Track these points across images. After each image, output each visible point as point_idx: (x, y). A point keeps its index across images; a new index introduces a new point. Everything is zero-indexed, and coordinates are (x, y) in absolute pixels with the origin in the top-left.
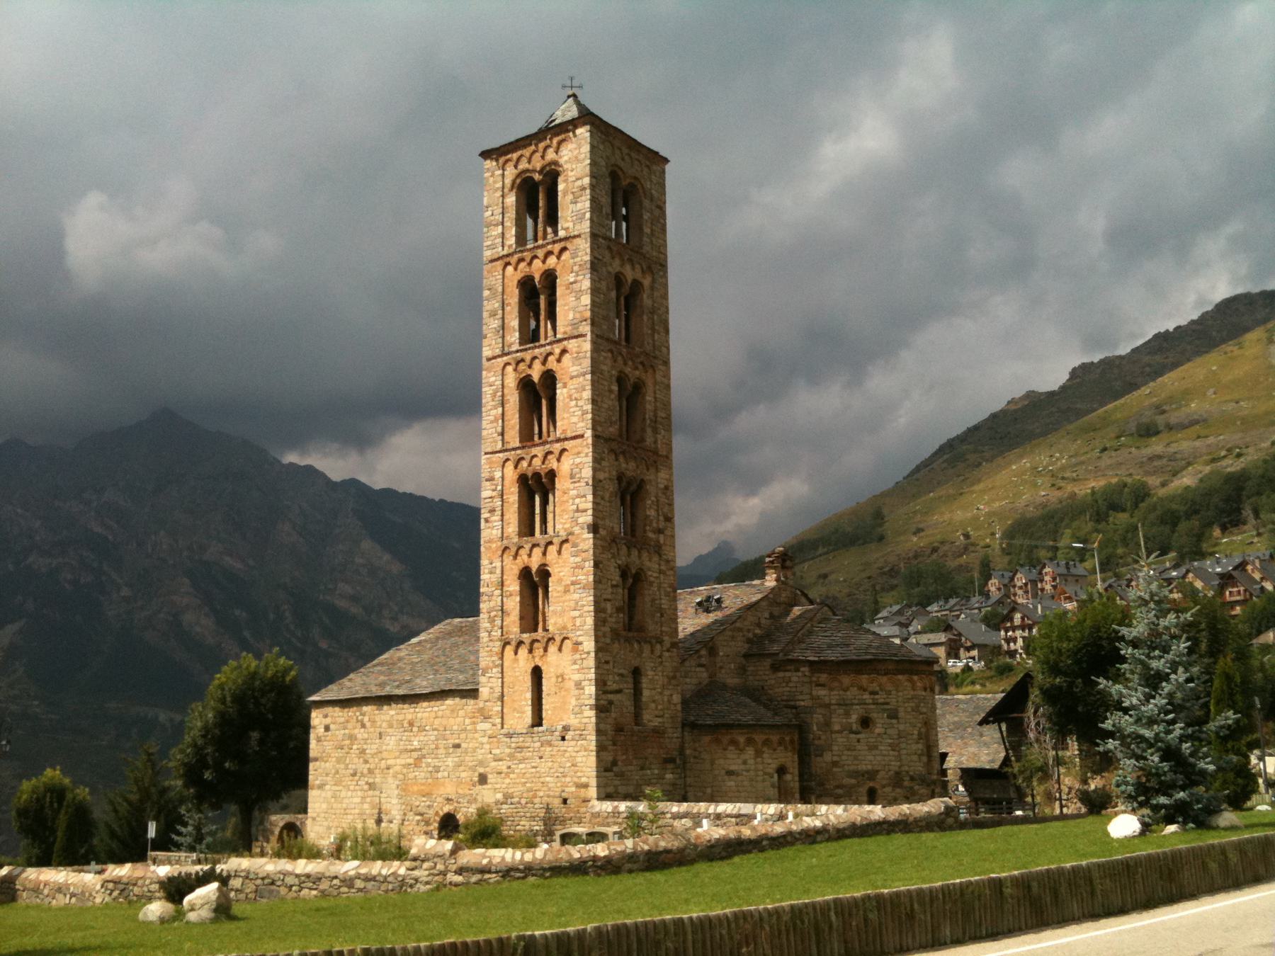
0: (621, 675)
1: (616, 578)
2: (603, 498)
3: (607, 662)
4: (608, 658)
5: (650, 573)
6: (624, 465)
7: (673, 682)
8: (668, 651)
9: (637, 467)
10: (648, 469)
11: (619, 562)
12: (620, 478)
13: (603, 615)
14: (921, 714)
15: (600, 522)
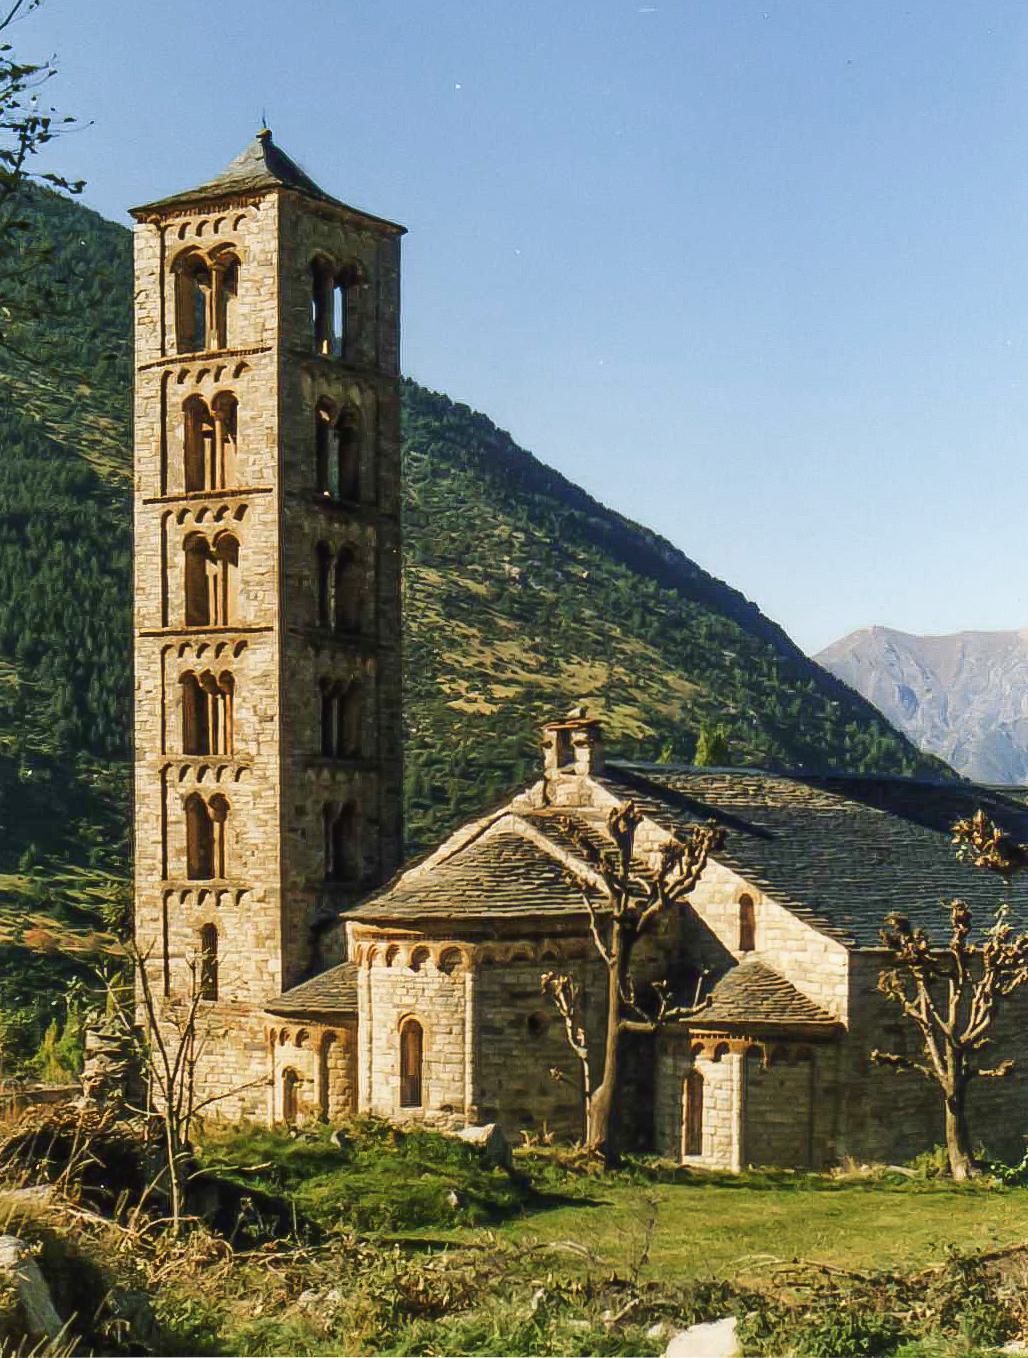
0: (186, 936)
1: (176, 811)
2: (150, 714)
3: (156, 920)
4: (155, 915)
5: (234, 798)
6: (195, 660)
7: (268, 943)
8: (260, 901)
9: (217, 656)
10: (236, 654)
11: (182, 791)
12: (187, 678)
13: (150, 861)
14: (398, 1006)
15: (145, 744)
